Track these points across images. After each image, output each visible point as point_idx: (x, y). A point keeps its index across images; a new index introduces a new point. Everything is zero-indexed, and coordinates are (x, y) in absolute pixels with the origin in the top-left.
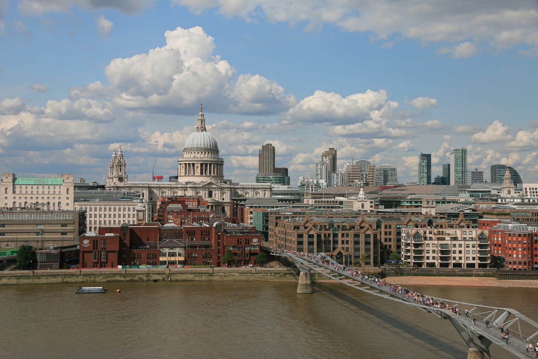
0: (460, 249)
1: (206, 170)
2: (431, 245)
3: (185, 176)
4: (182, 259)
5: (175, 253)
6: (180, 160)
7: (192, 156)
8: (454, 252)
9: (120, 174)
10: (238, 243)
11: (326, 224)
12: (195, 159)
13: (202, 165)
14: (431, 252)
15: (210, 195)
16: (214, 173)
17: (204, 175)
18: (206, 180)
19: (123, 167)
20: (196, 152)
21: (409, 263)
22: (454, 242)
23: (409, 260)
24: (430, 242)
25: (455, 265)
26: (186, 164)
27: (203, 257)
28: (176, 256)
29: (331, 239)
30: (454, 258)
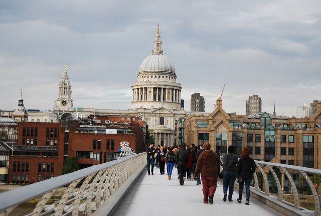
1: (159, 96)
3: (137, 102)
6: (133, 85)
7: (146, 79)
9: (64, 97)
10: (94, 148)
11: (255, 121)
13: (155, 89)
15: (162, 121)
16: (168, 99)
17: (157, 100)
18: (157, 105)
19: (67, 90)
20: (150, 76)
26: (138, 89)
29: (262, 145)
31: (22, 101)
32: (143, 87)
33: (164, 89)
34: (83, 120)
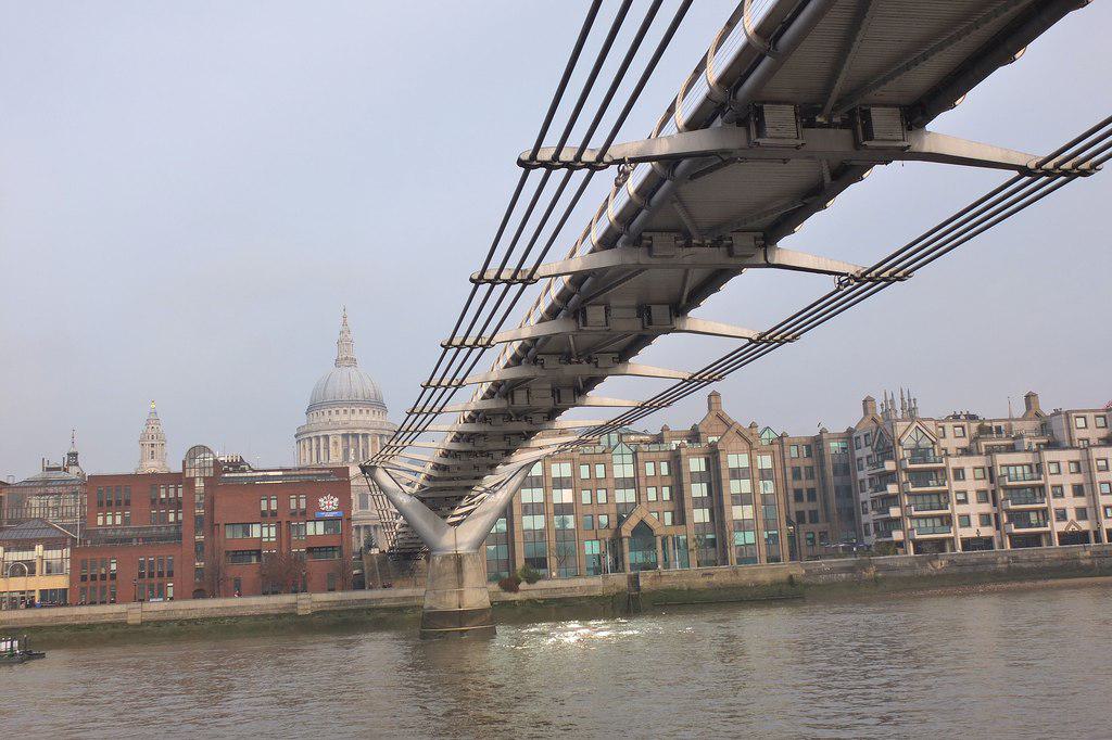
0: (1078, 479)
2: (969, 473)
4: (60, 582)
5: (31, 564)
8: (1059, 492)
12: (330, 426)
14: (972, 497)
20: (333, 411)
21: (900, 544)
22: (1049, 456)
23: (897, 535)
24: (968, 463)
25: (1066, 538)
26: (310, 439)
27: (141, 575)
28: (32, 572)
30: (1062, 515)
31: (75, 455)
32: (321, 434)
33: (365, 436)
34: (230, 464)
